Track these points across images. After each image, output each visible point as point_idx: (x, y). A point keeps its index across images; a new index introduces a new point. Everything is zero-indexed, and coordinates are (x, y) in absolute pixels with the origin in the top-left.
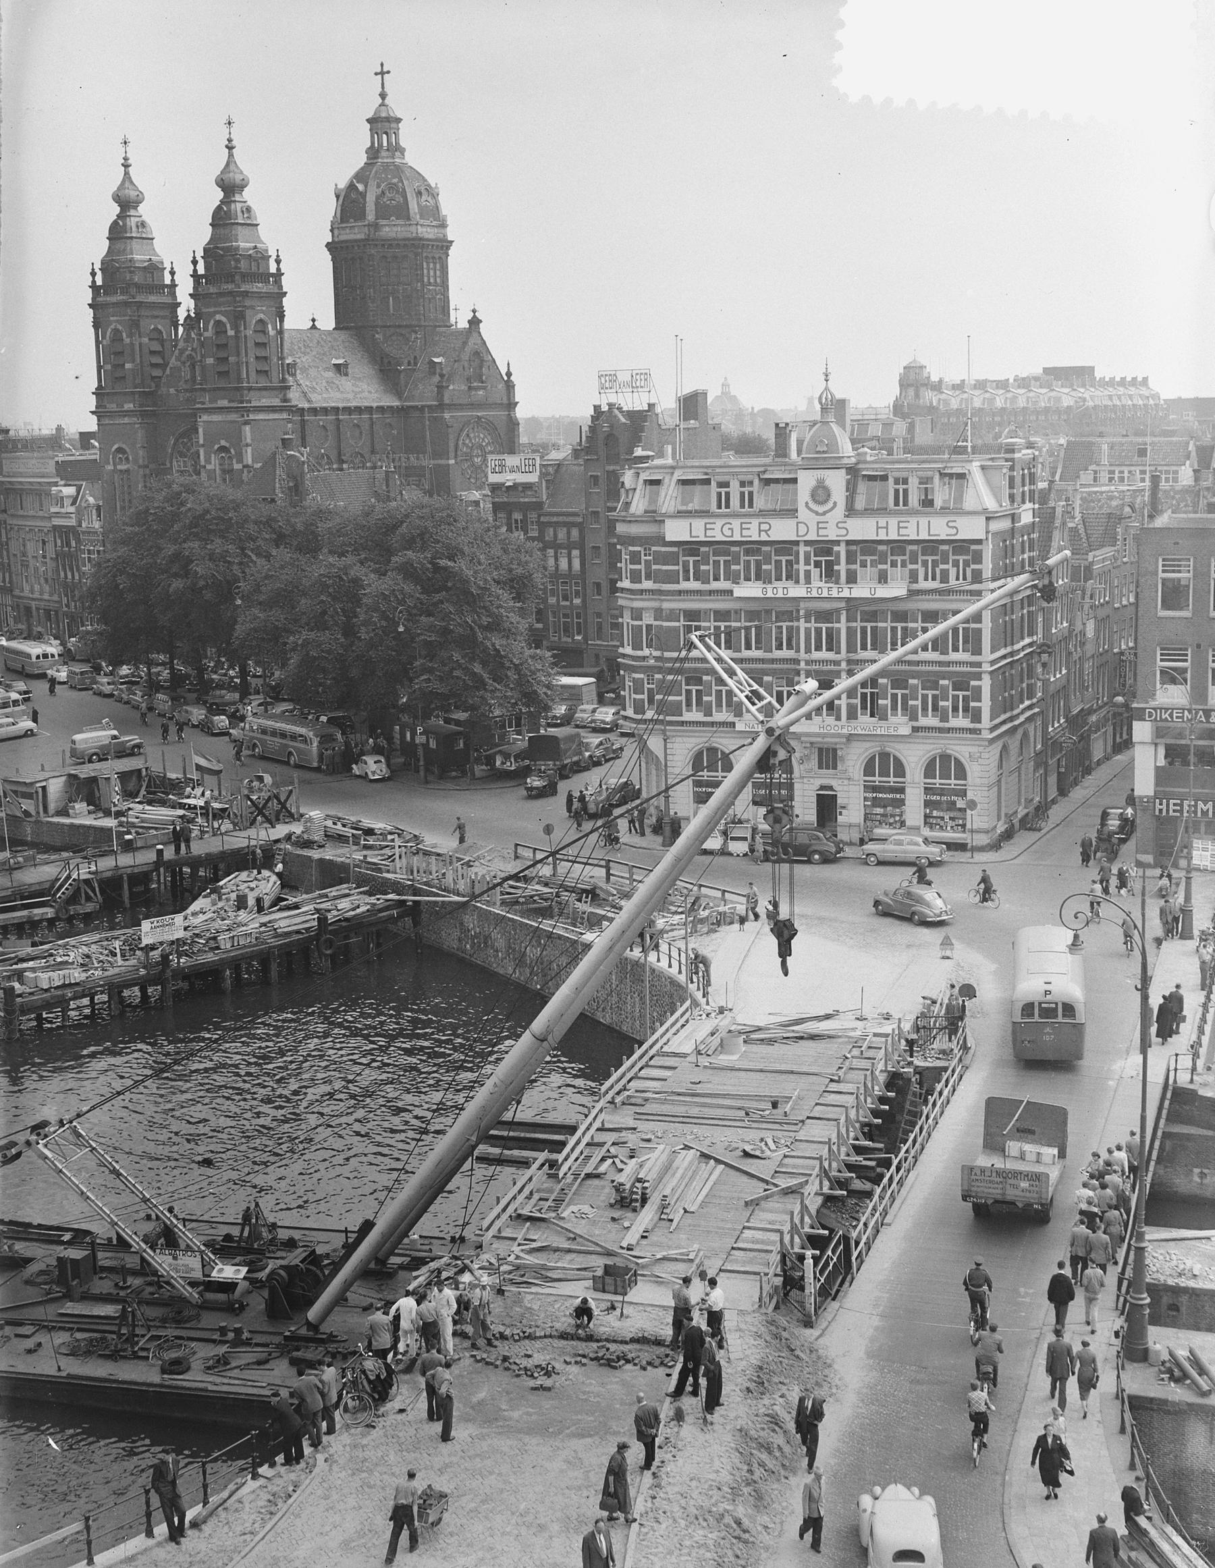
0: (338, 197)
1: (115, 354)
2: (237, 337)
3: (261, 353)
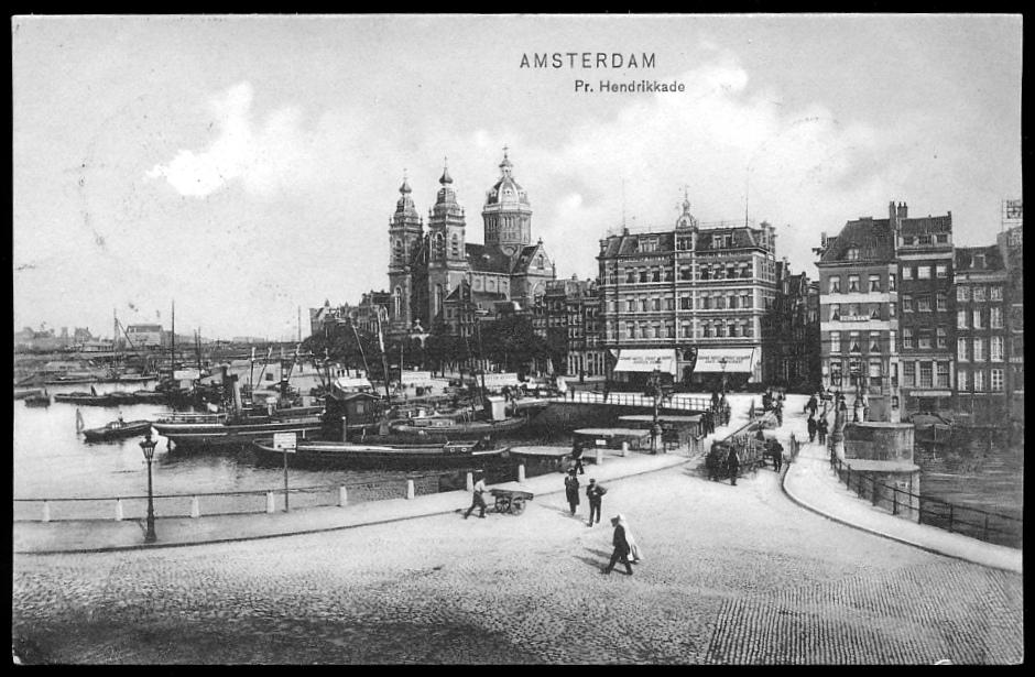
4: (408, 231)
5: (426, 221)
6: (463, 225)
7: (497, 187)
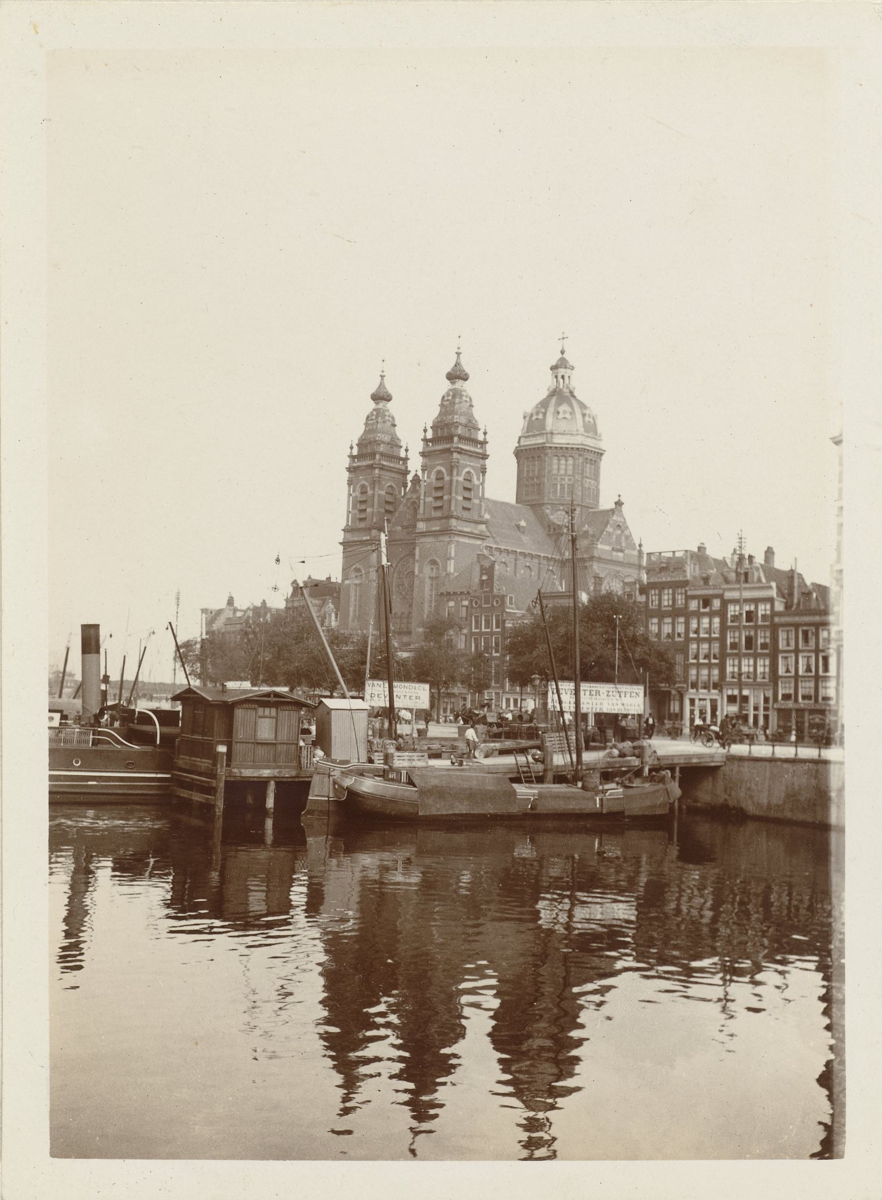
0: (525, 417)
1: (362, 502)
2: (451, 481)
3: (467, 494)
4: (382, 468)
5: (420, 446)
6: (485, 457)
7: (544, 404)
